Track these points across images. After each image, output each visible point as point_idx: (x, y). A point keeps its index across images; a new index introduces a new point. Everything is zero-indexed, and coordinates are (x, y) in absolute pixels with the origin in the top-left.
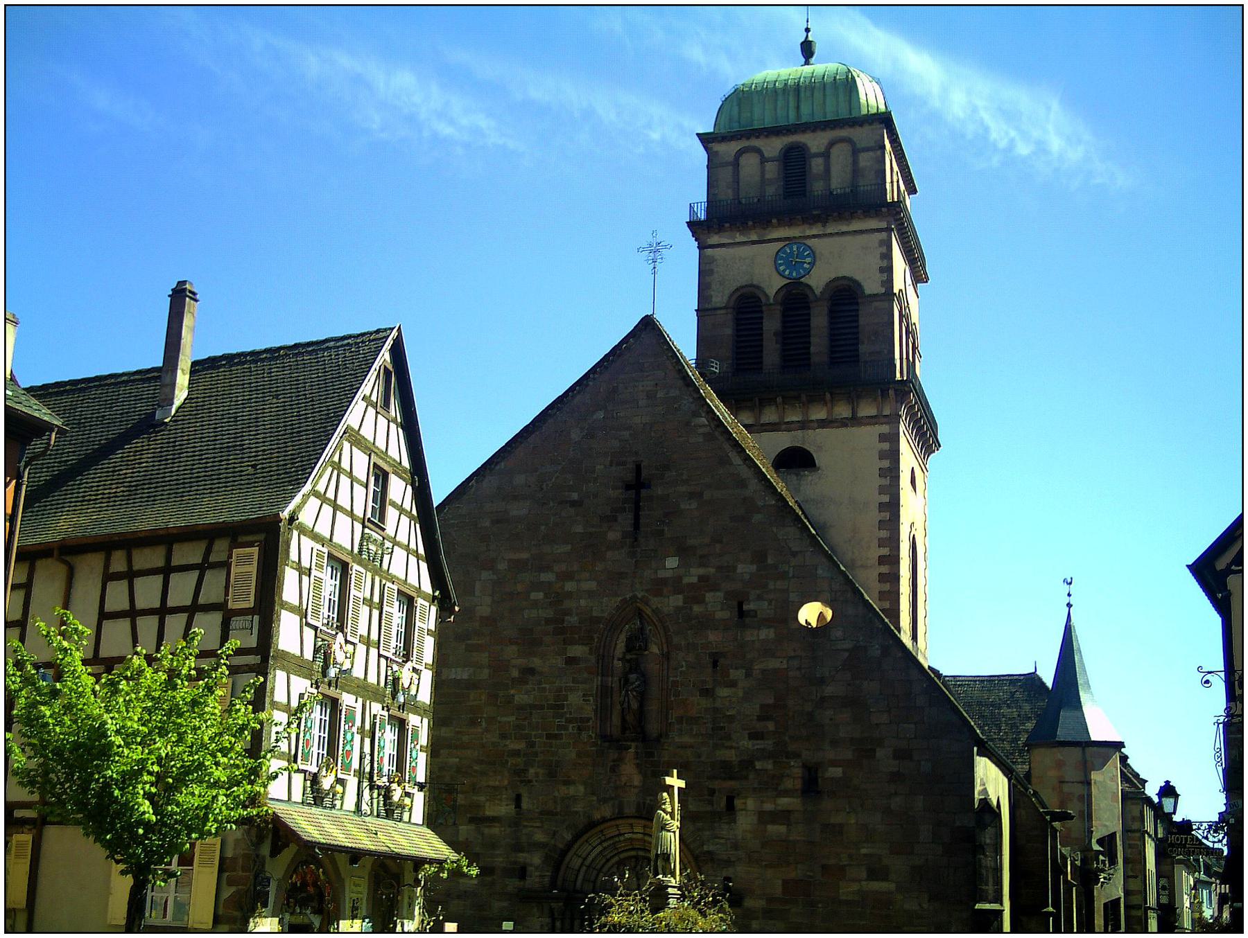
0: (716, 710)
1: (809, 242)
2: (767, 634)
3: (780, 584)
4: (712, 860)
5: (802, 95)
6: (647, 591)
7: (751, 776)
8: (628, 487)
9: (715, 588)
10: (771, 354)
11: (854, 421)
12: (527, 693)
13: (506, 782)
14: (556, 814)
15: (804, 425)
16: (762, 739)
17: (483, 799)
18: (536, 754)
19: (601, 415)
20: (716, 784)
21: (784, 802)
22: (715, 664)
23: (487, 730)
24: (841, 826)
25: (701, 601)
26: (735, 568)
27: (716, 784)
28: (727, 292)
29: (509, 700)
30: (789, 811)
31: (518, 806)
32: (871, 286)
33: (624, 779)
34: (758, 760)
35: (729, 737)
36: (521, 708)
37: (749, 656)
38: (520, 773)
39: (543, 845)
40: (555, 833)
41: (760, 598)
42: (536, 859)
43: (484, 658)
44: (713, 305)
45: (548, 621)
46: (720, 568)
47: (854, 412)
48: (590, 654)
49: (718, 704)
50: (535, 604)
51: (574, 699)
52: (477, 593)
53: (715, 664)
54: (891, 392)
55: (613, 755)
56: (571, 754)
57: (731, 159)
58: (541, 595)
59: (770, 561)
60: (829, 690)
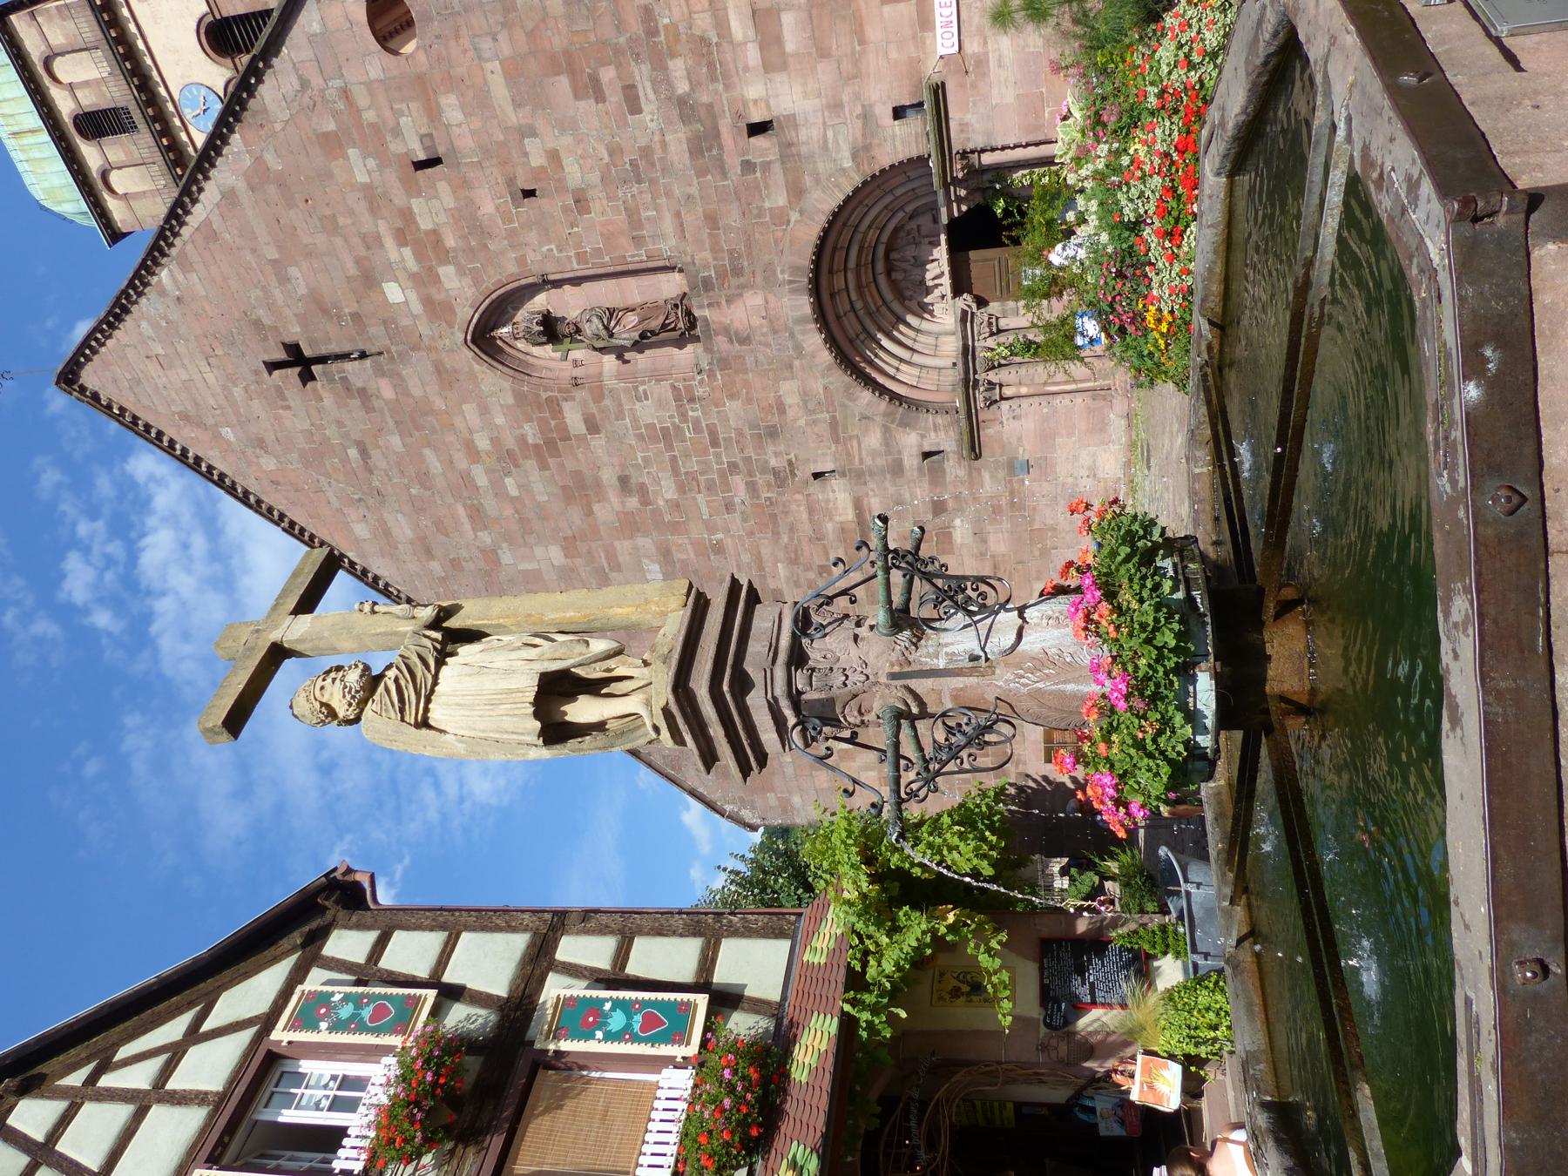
1: (176, 98)
3: (362, 100)
4: (867, 148)
5: (16, 129)
6: (451, 326)
7: (705, 99)
8: (307, 377)
9: (408, 216)
13: (798, 496)
14: (834, 418)
16: (633, 87)
17: (830, 526)
18: (747, 460)
19: (227, 433)
20: (733, 162)
22: (529, 194)
23: (727, 531)
25: (435, 234)
26: (368, 189)
27: (733, 162)
30: (754, 12)
33: (756, 321)
35: (646, 152)
36: (681, 489)
37: (501, 138)
38: (781, 478)
39: (886, 430)
41: (397, 132)
42: (910, 442)
43: (623, 547)
45: (544, 466)
48: (573, 399)
49: (595, 177)
51: (647, 413)
53: (529, 194)
55: (721, 342)
56: (733, 407)
57: (121, 204)
58: (509, 481)
59: (331, 126)
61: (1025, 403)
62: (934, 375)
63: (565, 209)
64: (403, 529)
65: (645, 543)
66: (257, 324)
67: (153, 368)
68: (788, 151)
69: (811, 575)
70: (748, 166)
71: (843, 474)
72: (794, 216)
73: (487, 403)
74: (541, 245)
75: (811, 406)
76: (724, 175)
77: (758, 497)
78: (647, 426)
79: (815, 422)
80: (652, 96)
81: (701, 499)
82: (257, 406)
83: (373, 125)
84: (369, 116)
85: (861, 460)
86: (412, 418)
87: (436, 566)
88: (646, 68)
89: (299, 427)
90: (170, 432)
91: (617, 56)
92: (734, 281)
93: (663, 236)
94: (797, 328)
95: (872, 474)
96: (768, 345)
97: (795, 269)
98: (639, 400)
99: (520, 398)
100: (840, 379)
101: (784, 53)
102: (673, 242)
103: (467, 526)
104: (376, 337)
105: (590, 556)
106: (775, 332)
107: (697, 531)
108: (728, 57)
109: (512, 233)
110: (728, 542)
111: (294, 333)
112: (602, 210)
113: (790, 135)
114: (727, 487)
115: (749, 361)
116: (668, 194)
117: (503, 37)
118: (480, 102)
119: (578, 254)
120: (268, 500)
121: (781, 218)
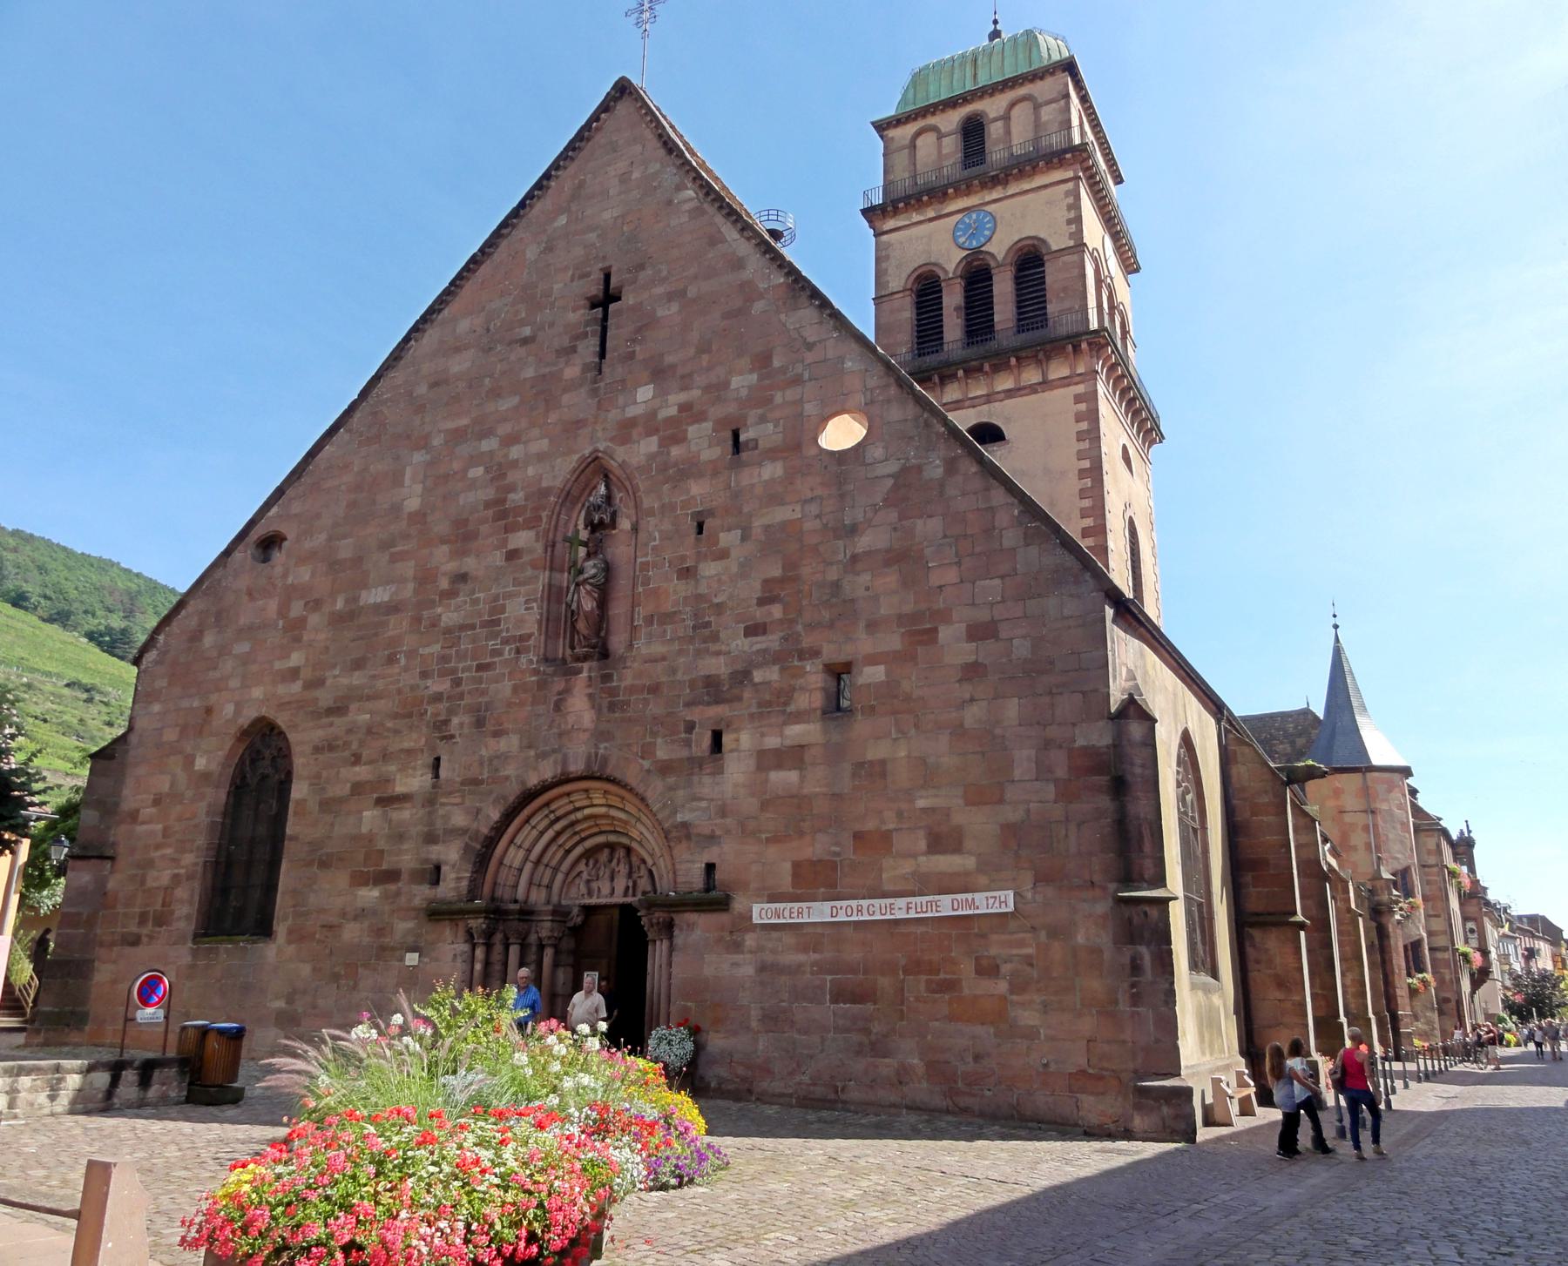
0: (699, 598)
1: (989, 208)
2: (772, 470)
3: (791, 394)
4: (688, 837)
5: (979, 62)
6: (612, 439)
7: (746, 695)
9: (700, 418)
10: (953, 328)
11: (1046, 385)
12: (458, 608)
15: (989, 398)
16: (764, 632)
17: (393, 768)
18: (461, 696)
20: (695, 714)
21: (796, 732)
22: (700, 528)
23: (406, 669)
24: (883, 762)
25: (679, 439)
26: (727, 384)
27: (695, 714)
28: (904, 276)
29: (434, 624)
30: (802, 747)
31: (437, 776)
32: (1057, 241)
33: (571, 719)
34: (759, 666)
35: (715, 637)
36: (448, 631)
37: (746, 510)
38: (441, 725)
39: (464, 831)
40: (478, 811)
41: (763, 419)
42: (451, 854)
43: (408, 568)
44: (890, 290)
45: (487, 505)
46: (707, 389)
47: (1044, 375)
48: (537, 540)
49: (703, 589)
50: (473, 485)
52: (407, 482)
53: (700, 528)
54: (1084, 346)
55: (559, 684)
56: (505, 688)
57: (907, 142)
58: (480, 471)
59: (776, 363)
60: (864, 542)
61: (466, 967)
62: (511, 881)
63: (683, 558)
64: (458, 365)
65: (408, 591)
66: (641, 267)
67: (622, 165)
68: (695, 764)
69: (354, 746)
70: (690, 727)
71: (434, 786)
72: (646, 764)
73: (545, 466)
74: (660, 532)
75: (495, 762)
76: (688, 705)
77: (429, 703)
78: (504, 606)
79: (481, 764)
80: (755, 648)
81: (436, 648)
82: (579, 252)
83: (770, 400)
84: (778, 399)
85: (443, 804)
86: (545, 392)
87: (422, 389)
88: (776, 646)
89: (556, 287)
90: (572, 168)
91: (788, 622)
92: (605, 703)
93: (649, 643)
94: (559, 756)
95: (430, 813)
96: (550, 727)
97: (605, 760)
98: (526, 602)
99: (544, 493)
100: (512, 791)
101: (770, 769)
102: (644, 651)
103: (450, 425)
104: (614, 370)
105: (406, 536)
106: (560, 735)
107: (409, 641)
108: (773, 720)
109: (673, 507)
110: (396, 669)
111: (629, 299)
112: (677, 590)
113: (708, 769)
114: (442, 674)
115: (541, 709)
116: (681, 652)
117: (817, 524)
118: (774, 498)
119: (647, 563)
120: (504, 244)
121: (648, 751)
